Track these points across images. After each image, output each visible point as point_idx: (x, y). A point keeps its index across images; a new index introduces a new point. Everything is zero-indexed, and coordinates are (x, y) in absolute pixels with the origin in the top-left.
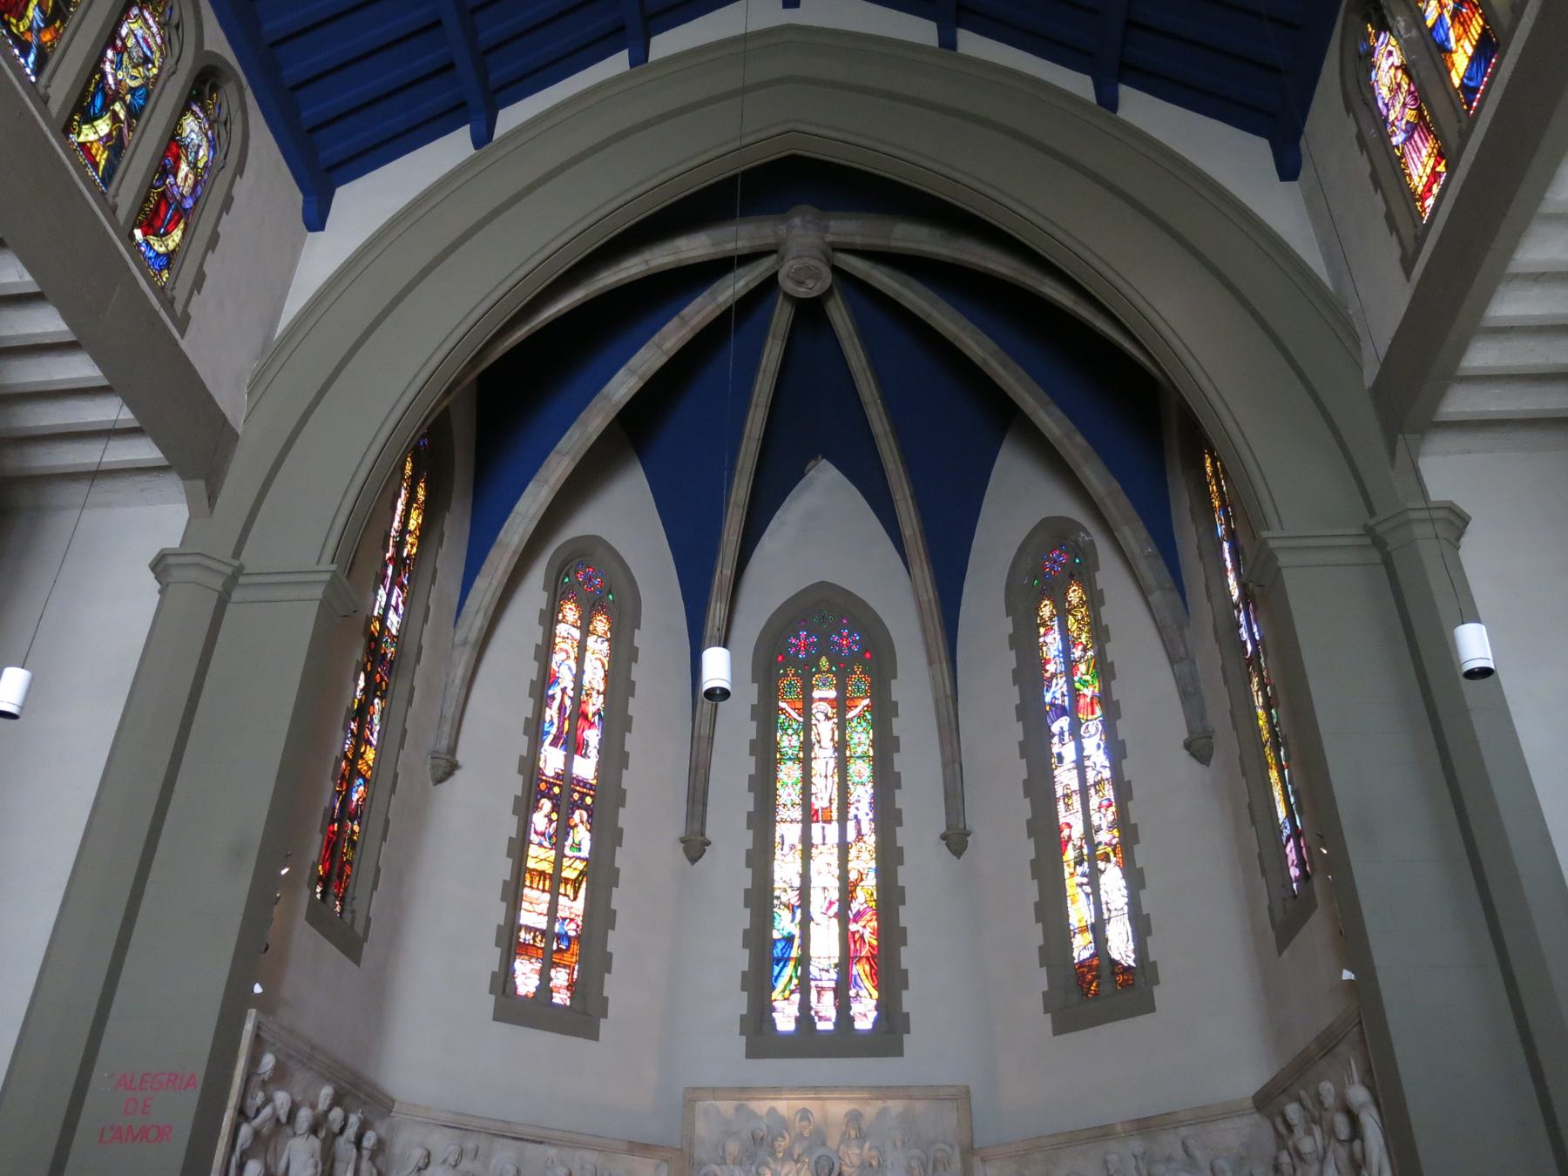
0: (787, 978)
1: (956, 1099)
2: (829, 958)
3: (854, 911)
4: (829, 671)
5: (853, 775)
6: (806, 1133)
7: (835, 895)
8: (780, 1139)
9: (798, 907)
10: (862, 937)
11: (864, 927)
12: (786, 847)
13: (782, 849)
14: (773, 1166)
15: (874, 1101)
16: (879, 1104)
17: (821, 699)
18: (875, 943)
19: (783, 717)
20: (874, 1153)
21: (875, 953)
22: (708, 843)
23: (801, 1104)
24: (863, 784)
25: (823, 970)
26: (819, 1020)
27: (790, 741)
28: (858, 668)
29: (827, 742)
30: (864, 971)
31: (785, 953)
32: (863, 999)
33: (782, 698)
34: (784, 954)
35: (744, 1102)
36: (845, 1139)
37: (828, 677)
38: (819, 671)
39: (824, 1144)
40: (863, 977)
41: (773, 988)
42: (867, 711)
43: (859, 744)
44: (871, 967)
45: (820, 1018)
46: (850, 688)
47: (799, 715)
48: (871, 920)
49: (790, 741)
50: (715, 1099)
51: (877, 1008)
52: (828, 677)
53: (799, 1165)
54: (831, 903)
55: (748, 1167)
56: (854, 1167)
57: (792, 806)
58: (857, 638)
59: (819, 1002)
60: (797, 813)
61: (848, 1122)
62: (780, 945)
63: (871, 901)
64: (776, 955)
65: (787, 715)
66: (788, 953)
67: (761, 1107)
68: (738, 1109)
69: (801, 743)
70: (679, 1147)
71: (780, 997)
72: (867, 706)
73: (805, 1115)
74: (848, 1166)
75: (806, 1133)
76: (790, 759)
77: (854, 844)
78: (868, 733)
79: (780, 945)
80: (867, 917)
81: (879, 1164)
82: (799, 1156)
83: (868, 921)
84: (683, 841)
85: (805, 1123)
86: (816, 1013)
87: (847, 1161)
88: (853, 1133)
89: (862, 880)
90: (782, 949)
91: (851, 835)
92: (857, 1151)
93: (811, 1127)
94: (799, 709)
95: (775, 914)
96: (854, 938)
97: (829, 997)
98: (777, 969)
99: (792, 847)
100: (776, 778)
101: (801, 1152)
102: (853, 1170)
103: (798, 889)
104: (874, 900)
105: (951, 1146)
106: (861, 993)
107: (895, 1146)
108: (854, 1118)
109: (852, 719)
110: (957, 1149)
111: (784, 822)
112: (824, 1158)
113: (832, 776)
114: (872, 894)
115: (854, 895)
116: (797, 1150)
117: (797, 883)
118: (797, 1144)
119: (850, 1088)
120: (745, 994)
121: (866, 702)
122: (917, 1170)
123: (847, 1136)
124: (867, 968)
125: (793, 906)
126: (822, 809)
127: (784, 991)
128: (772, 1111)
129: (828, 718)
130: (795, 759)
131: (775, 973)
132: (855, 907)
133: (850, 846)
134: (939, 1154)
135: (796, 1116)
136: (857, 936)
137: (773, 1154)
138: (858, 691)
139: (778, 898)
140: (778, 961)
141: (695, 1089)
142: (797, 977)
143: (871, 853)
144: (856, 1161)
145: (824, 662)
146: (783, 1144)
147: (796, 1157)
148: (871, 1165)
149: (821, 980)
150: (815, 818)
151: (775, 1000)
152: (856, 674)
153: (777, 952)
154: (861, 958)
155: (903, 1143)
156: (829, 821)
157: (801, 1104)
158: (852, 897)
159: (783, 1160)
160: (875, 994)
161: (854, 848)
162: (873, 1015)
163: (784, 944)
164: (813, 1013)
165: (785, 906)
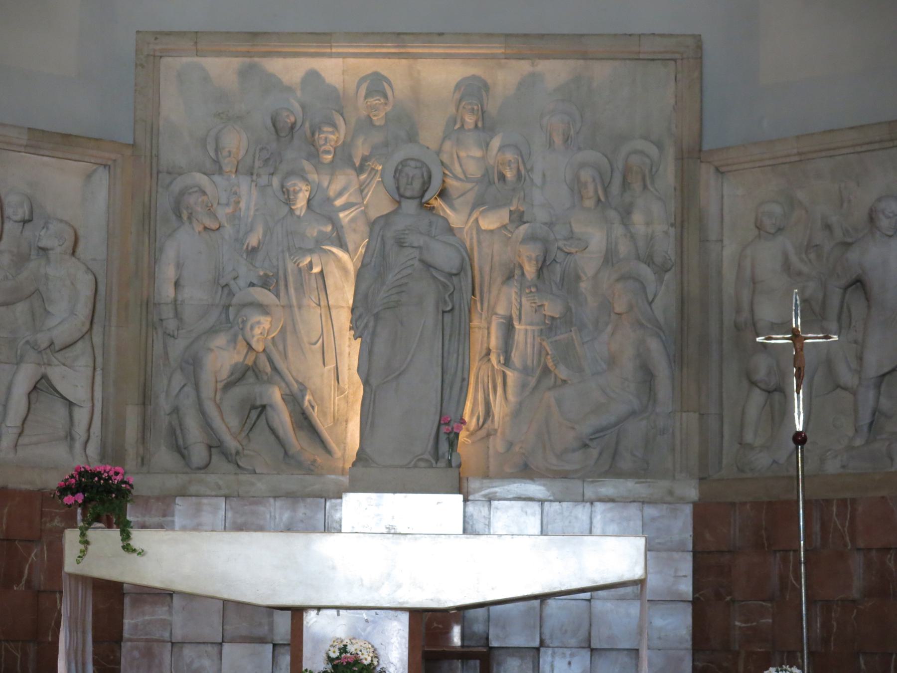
1: (675, 60)
6: (378, 120)
14: (313, 177)
15: (513, 63)
16: (525, 67)
20: (510, 156)
23: (368, 66)
35: (256, 59)
39: (412, 138)
53: (363, 177)
55: (264, 180)
56: (468, 180)
61: (460, 101)
70: (131, 142)
81: (519, 176)
82: (365, 159)
85: (375, 101)
87: (458, 170)
88: (470, 120)
92: (477, 153)
93: (389, 108)
101: (367, 153)
102: (469, 186)
105: (660, 146)
107: (551, 143)
110: (671, 152)
112: (412, 163)
116: (361, 150)
118: (360, 141)
119: (466, 37)
122: (591, 188)
128: (313, 76)
134: (635, 160)
135: (358, 87)
137: (314, 155)
141: (158, 35)
144: (474, 170)
147: (357, 162)
148: (502, 177)
155: (567, 139)
157: (368, 66)
159: (333, 167)
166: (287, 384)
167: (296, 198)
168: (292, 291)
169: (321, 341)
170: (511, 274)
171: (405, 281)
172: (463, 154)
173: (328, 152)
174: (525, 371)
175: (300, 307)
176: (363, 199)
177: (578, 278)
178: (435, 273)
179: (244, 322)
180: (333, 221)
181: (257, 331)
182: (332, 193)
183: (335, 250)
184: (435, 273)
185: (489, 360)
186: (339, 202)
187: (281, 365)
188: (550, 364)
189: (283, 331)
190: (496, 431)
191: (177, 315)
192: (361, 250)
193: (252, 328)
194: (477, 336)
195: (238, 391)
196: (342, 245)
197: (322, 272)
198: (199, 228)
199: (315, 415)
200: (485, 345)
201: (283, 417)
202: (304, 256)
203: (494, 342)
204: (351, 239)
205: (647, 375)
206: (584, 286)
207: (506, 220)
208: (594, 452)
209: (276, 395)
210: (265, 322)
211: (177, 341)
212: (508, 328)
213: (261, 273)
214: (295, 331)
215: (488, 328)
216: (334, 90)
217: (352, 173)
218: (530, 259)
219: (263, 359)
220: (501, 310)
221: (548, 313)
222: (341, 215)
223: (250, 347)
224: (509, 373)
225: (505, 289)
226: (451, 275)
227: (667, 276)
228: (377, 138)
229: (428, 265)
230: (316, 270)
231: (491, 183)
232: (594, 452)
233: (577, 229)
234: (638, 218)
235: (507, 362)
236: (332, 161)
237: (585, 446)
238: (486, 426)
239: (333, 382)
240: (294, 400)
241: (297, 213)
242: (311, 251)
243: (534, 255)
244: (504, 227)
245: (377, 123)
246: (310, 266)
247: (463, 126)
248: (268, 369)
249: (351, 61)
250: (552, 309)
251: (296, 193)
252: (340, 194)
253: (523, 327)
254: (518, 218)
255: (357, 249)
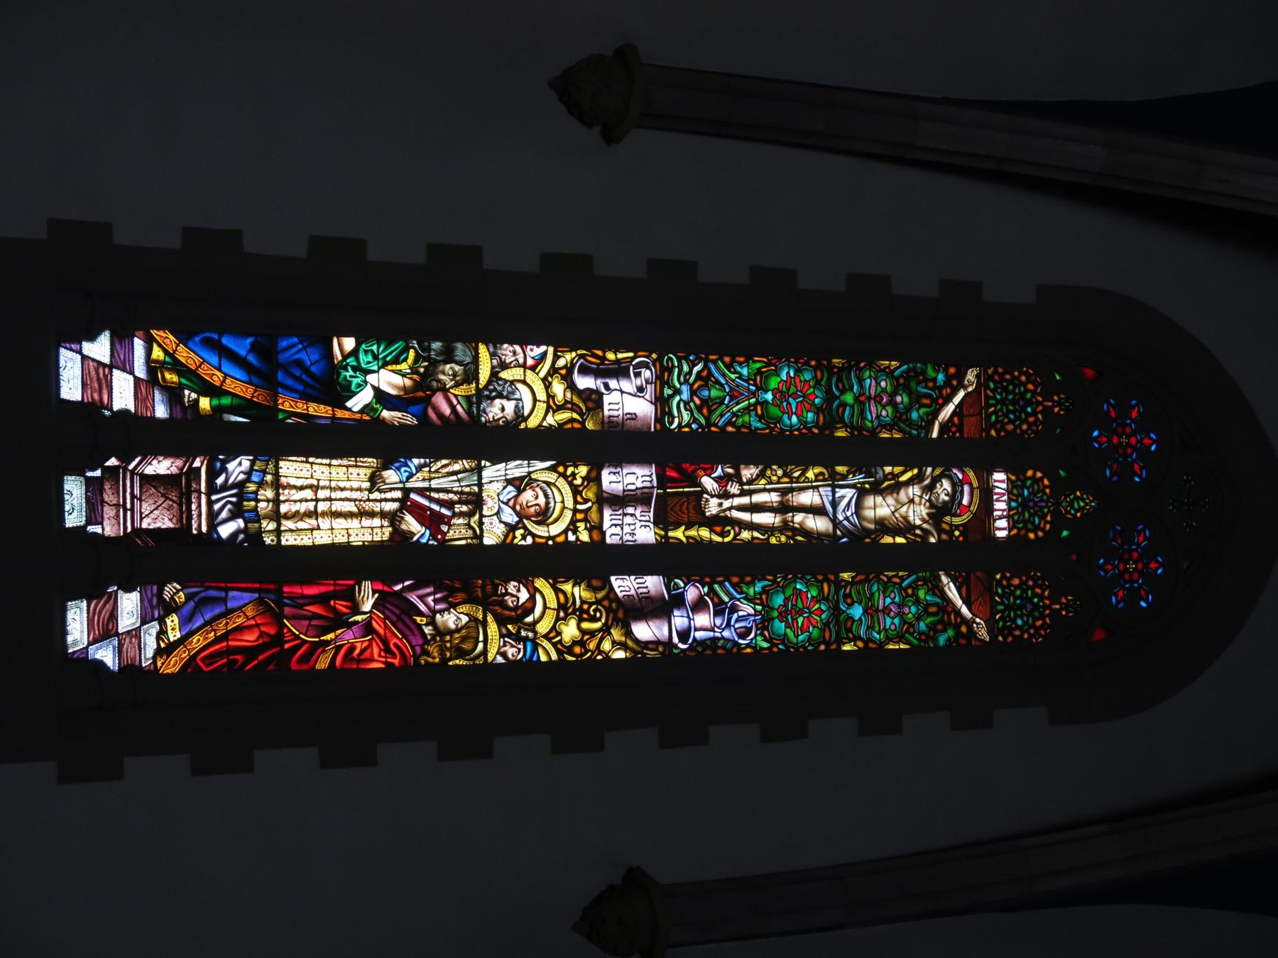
0: (217, 378)
2: (277, 516)
3: (413, 598)
4: (1060, 521)
5: (789, 592)
7: (458, 533)
9: (423, 418)
10: (340, 621)
11: (368, 628)
12: (584, 382)
13: (584, 371)
17: (986, 494)
18: (322, 663)
19: (941, 377)
21: (294, 665)
22: (611, 136)
24: (764, 623)
25: (241, 496)
26: (89, 481)
27: (878, 398)
28: (1066, 607)
29: (880, 508)
30: (240, 629)
31: (289, 374)
32: (154, 628)
33: (991, 378)
34: (286, 369)
37: (1043, 517)
38: (1060, 488)
40: (221, 627)
41: (183, 338)
42: (959, 634)
43: (870, 611)
44: (250, 652)
45: (94, 492)
46: (1016, 581)
47: (944, 427)
48: (387, 650)
49: (878, 398)
51: (130, 670)
52: (1043, 517)
54: (432, 521)
57: (705, 402)
58: (1143, 604)
59: (147, 480)
60: (682, 417)
62: (310, 357)
63: (442, 650)
64: (284, 344)
65: (947, 391)
66: (289, 382)
69: (873, 432)
71: (157, 353)
72: (972, 633)
76: (830, 398)
77: (600, 595)
78: (900, 638)
79: (310, 357)
80: (396, 638)
83: (385, 641)
84: (625, 55)
86: (112, 473)
89: (501, 622)
90: (299, 363)
91: (623, 585)
94: (960, 428)
95: (399, 345)
96: (336, 595)
97: (157, 518)
98: (241, 347)
99: (593, 400)
100: (777, 354)
103: (474, 418)
104: (444, 661)
106: (173, 621)
109: (939, 590)
111: (659, 377)
113: (786, 527)
114: (461, 653)
115: (460, 596)
117: (498, 410)
120: (173, 241)
121: (983, 634)
124: (250, 638)
125: (427, 401)
126: (699, 495)
127: (178, 367)
129: (939, 513)
130: (830, 414)
131: (227, 341)
132: (424, 600)
133: (595, 583)
136: (341, 606)
138: (1009, 607)
139: (449, 357)
140: (265, 350)
142: (217, 411)
143: (577, 650)
145: (1081, 504)
149: (212, 489)
150: (671, 473)
151: (149, 342)
152: (1054, 599)
153: (291, 348)
154: (278, 619)
156: (662, 521)
158: (452, 591)
160: (171, 666)
161: (587, 595)
162: (106, 655)
163: (313, 369)
164: (113, 462)
165: (424, 376)
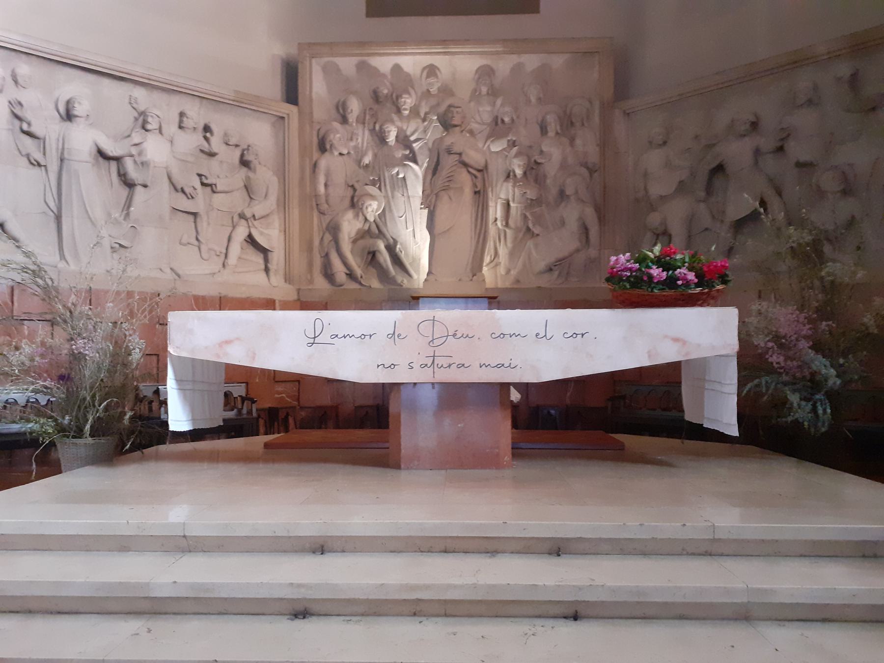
6: (434, 90)
8: (407, 96)
14: (399, 124)
16: (514, 59)
23: (427, 60)
36: (475, 95)
50: (332, 55)
53: (426, 123)
56: (484, 124)
61: (479, 78)
67: (384, 63)
68: (362, 67)
73: (431, 71)
74: (479, 123)
75: (434, 90)
81: (513, 120)
82: (426, 114)
85: (432, 80)
87: (478, 118)
88: (484, 90)
92: (489, 108)
93: (439, 85)
101: (427, 110)
102: (485, 127)
108: (485, 73)
116: (423, 110)
118: (423, 104)
122: (553, 124)
123: (477, 93)
128: (397, 68)
135: (422, 72)
137: (399, 111)
146: (409, 101)
147: (422, 115)
148: (503, 121)
157: (427, 60)
159: (409, 118)
166: (387, 240)
167: (388, 135)
168: (388, 187)
169: (404, 216)
170: (509, 175)
171: (452, 174)
172: (481, 109)
173: (405, 109)
174: (517, 230)
175: (393, 197)
176: (426, 135)
177: (545, 176)
178: (471, 170)
179: (363, 204)
180: (412, 151)
181: (370, 209)
182: (408, 133)
183: (411, 164)
184: (471, 170)
185: (496, 224)
186: (412, 138)
187: (384, 230)
188: (531, 226)
189: (384, 210)
190: (500, 263)
191: (327, 202)
192: (425, 165)
193: (367, 208)
194: (491, 211)
195: (361, 243)
196: (416, 162)
197: (404, 177)
198: (336, 153)
199: (403, 256)
200: (494, 216)
201: (385, 258)
202: (394, 166)
203: (499, 214)
204: (420, 158)
205: (585, 230)
206: (548, 181)
207: (505, 146)
208: (556, 273)
209: (381, 245)
210: (374, 205)
211: (326, 217)
212: (507, 206)
213: (371, 178)
214: (391, 211)
215: (496, 207)
216: (408, 75)
217: (420, 121)
218: (519, 166)
219: (374, 227)
220: (503, 196)
221: (529, 197)
222: (414, 145)
223: (366, 220)
224: (508, 231)
225: (505, 184)
226: (479, 171)
227: (596, 175)
228: (433, 101)
229: (465, 165)
230: (401, 176)
231: (497, 124)
232: (556, 273)
233: (544, 149)
234: (578, 142)
235: (507, 225)
236: (408, 116)
237: (551, 270)
238: (495, 260)
239: (412, 238)
240: (391, 249)
241: (390, 144)
242: (398, 165)
243: (522, 163)
244: (504, 149)
245: (432, 93)
246: (398, 174)
247: (480, 93)
248: (377, 232)
249: (418, 57)
250: (531, 194)
251: (389, 132)
252: (412, 134)
253: (515, 205)
254: (513, 144)
255: (423, 164)
